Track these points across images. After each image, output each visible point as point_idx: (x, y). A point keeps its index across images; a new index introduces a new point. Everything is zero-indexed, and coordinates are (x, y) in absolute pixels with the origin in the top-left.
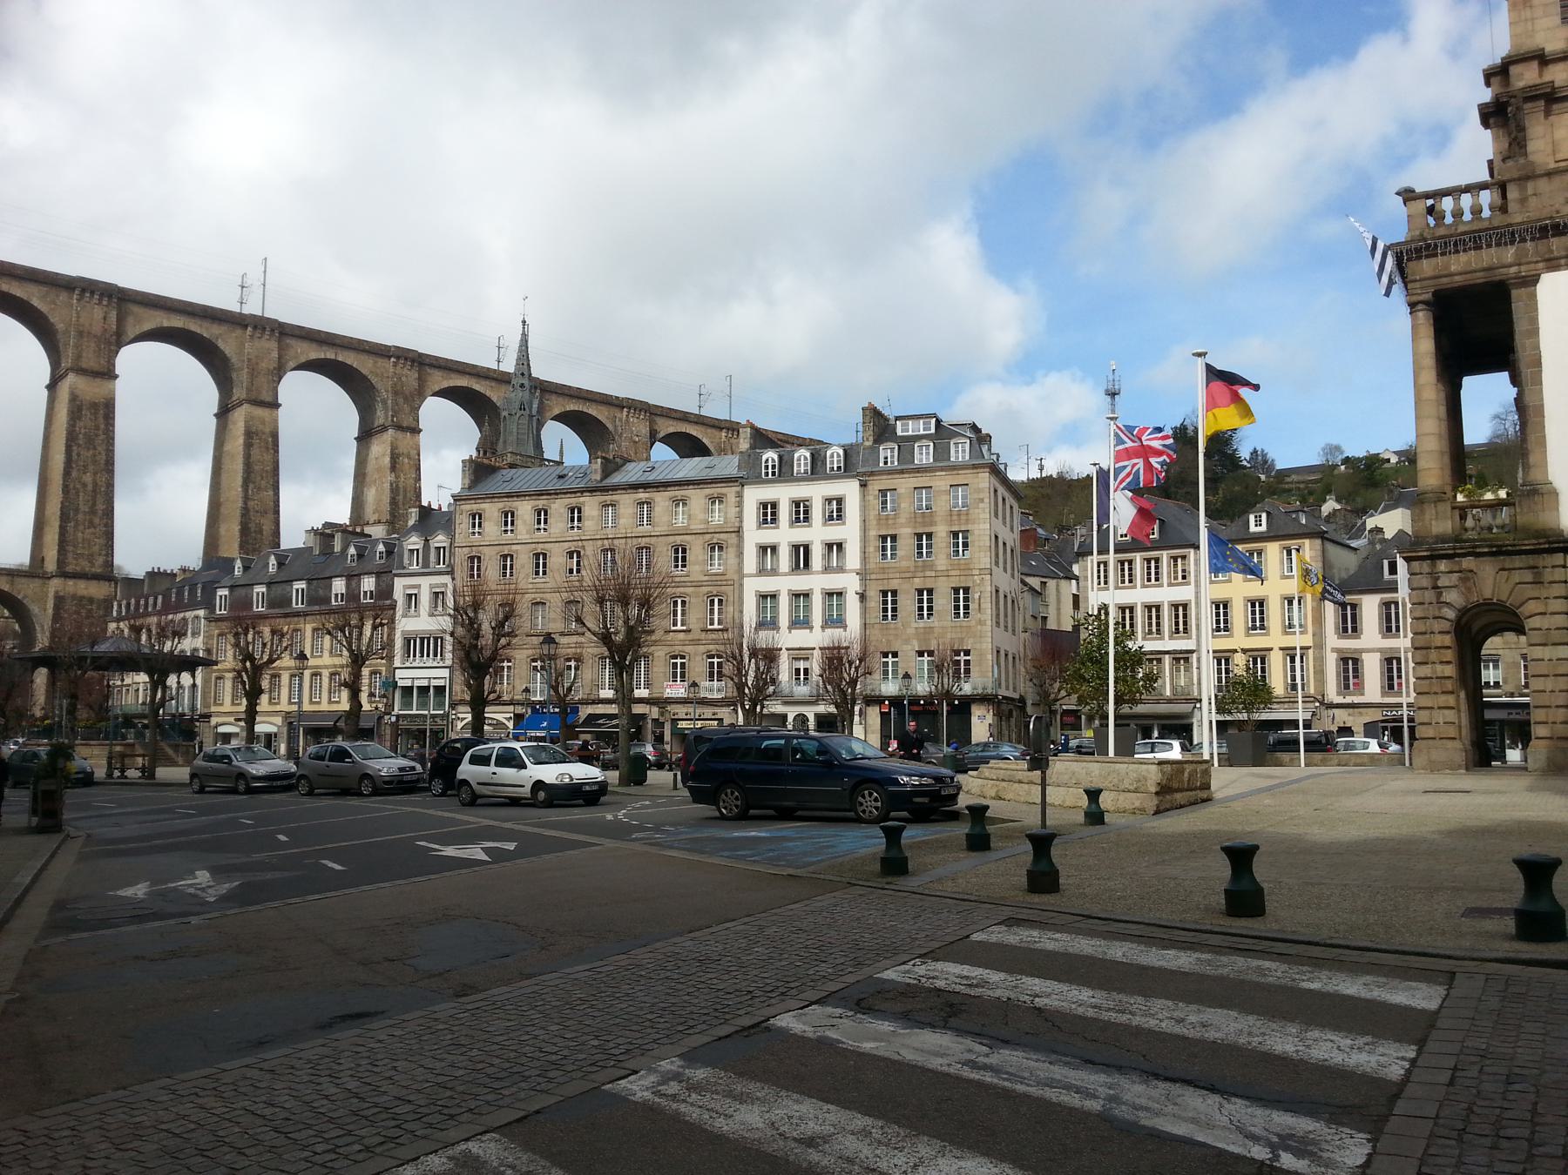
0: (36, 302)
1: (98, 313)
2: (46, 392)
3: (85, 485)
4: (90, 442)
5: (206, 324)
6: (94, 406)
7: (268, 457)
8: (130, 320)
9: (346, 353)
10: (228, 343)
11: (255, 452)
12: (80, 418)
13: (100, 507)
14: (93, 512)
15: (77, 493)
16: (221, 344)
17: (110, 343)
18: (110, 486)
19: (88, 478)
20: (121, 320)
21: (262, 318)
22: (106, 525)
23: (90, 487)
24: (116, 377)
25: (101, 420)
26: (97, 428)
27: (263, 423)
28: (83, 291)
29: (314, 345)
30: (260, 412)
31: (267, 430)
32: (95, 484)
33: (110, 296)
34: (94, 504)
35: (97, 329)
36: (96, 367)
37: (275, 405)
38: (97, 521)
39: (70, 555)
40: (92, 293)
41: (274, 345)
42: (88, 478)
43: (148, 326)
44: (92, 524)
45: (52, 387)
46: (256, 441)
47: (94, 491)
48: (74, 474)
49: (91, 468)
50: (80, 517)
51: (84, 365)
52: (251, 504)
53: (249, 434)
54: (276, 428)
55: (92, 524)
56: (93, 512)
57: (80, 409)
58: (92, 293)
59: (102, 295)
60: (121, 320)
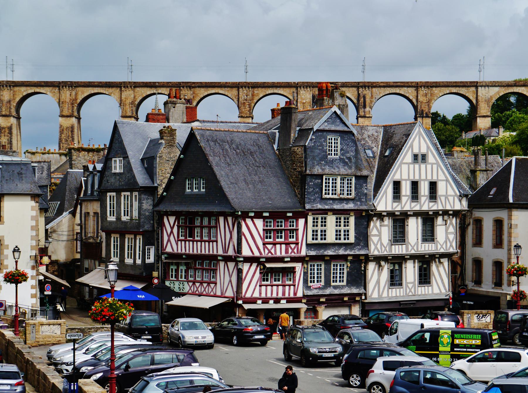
1: (68, 93)
5: (107, 89)
8: (80, 93)
9: (162, 89)
20: (76, 94)
25: (70, 133)
26: (69, 136)
28: (63, 87)
29: (149, 89)
33: (72, 87)
35: (68, 100)
40: (66, 87)
51: (64, 114)
57: (63, 130)
58: (66, 87)
59: (69, 87)
60: (76, 94)
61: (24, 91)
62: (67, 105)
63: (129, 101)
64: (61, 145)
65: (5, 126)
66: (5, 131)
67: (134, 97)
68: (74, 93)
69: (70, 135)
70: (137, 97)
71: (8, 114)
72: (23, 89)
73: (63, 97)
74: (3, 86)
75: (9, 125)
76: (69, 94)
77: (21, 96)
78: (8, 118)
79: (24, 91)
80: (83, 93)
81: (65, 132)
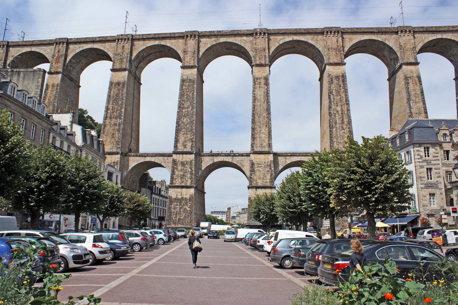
0: (310, 41)
1: (334, 39)
2: (319, 82)
3: (337, 111)
4: (338, 92)
6: (337, 77)
7: (418, 88)
10: (391, 41)
11: (411, 86)
12: (332, 83)
13: (346, 120)
14: (343, 122)
15: (335, 115)
16: (387, 42)
17: (341, 51)
18: (348, 110)
19: (339, 108)
21: (403, 27)
22: (349, 128)
23: (340, 112)
24: (345, 64)
25: (341, 83)
26: (340, 86)
27: (412, 72)
28: (327, 32)
30: (410, 68)
31: (415, 75)
32: (342, 110)
33: (338, 32)
34: (343, 120)
35: (335, 46)
36: (336, 61)
37: (417, 64)
38: (345, 126)
39: (335, 144)
40: (331, 32)
41: (411, 37)
42: (339, 108)
43: (354, 42)
44: (343, 129)
45: (321, 79)
46: (410, 81)
47: (342, 113)
48: (333, 107)
49: (339, 104)
50: (338, 126)
52: (412, 110)
53: (406, 78)
54: (419, 73)
55: (343, 129)
56: (343, 122)
57: (332, 80)
58: (331, 32)
59: (335, 32)
61: (281, 39)
62: (334, 53)
63: (409, 46)
64: (332, 96)
65: (260, 77)
66: (260, 83)
67: (415, 43)
68: (340, 39)
69: (342, 85)
70: (417, 44)
71: (263, 63)
72: (279, 37)
73: (328, 44)
74: (256, 34)
75: (265, 75)
76: (336, 40)
77: (277, 45)
78: (263, 68)
79: (281, 39)
80: (351, 40)
81: (335, 81)
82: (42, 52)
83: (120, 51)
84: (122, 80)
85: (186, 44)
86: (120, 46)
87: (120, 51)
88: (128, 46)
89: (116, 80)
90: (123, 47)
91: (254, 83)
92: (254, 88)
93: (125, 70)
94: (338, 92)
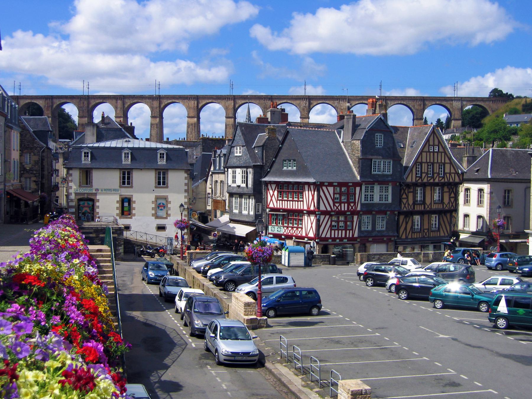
6: (192, 124)
35: (192, 106)
68: (196, 102)
81: (191, 127)
82: (37, 103)
83: (82, 105)
84: (84, 123)
85: (117, 103)
86: (82, 102)
87: (82, 105)
88: (86, 102)
89: (81, 122)
90: (83, 103)
91: (151, 127)
92: (151, 129)
93: (85, 117)
94: (191, 132)
